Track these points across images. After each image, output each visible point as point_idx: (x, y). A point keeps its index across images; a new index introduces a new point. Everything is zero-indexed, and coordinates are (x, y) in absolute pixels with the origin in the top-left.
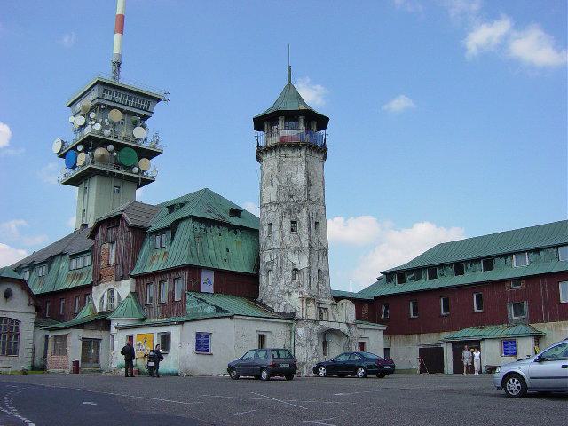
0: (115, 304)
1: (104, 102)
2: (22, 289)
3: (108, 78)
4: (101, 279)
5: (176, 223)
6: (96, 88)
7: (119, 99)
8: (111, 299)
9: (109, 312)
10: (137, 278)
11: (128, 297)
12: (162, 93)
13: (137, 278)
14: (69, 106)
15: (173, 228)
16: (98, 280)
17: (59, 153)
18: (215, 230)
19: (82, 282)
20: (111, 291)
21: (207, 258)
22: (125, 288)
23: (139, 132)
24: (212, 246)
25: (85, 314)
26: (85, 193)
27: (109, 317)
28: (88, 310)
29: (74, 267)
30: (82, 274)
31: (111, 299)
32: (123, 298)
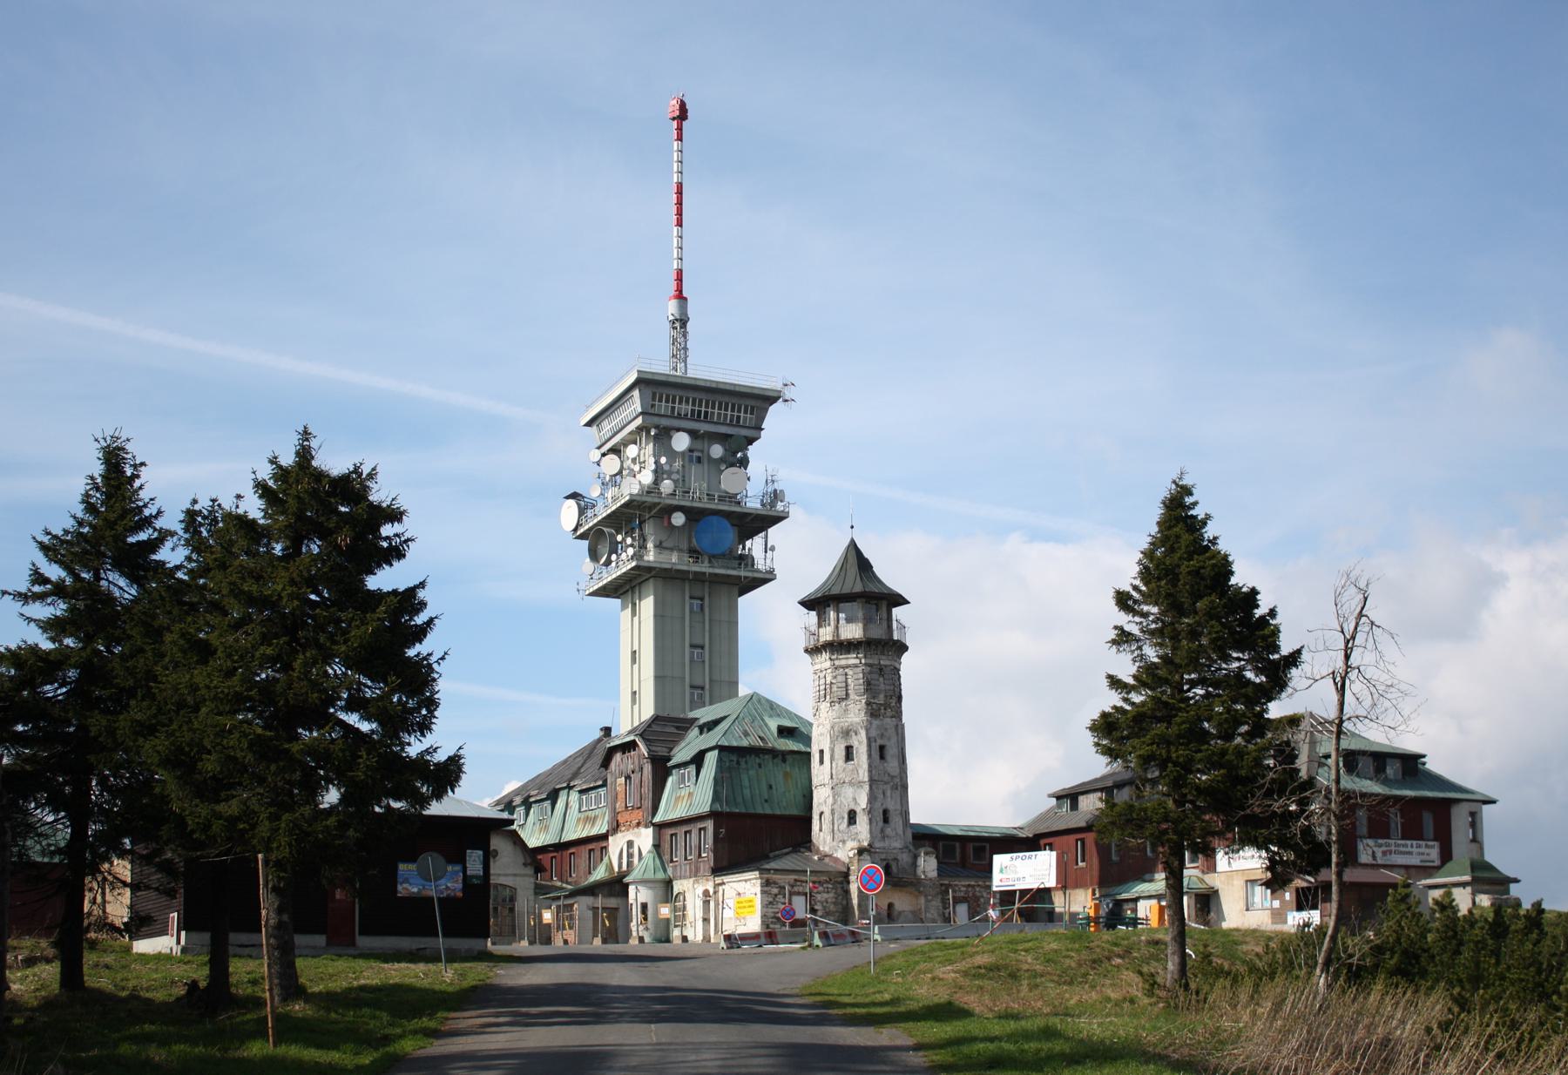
0: (636, 860)
1: (656, 420)
2: (515, 843)
3: (661, 365)
4: (618, 826)
6: (636, 393)
7: (686, 408)
8: (630, 856)
9: (623, 875)
12: (779, 386)
14: (589, 424)
16: (615, 828)
17: (575, 530)
18: (753, 760)
19: (594, 831)
20: (630, 844)
21: (739, 799)
22: (644, 839)
23: (729, 480)
24: (746, 783)
25: (600, 874)
26: (634, 614)
27: (626, 880)
30: (595, 818)
31: (630, 856)
32: (644, 853)
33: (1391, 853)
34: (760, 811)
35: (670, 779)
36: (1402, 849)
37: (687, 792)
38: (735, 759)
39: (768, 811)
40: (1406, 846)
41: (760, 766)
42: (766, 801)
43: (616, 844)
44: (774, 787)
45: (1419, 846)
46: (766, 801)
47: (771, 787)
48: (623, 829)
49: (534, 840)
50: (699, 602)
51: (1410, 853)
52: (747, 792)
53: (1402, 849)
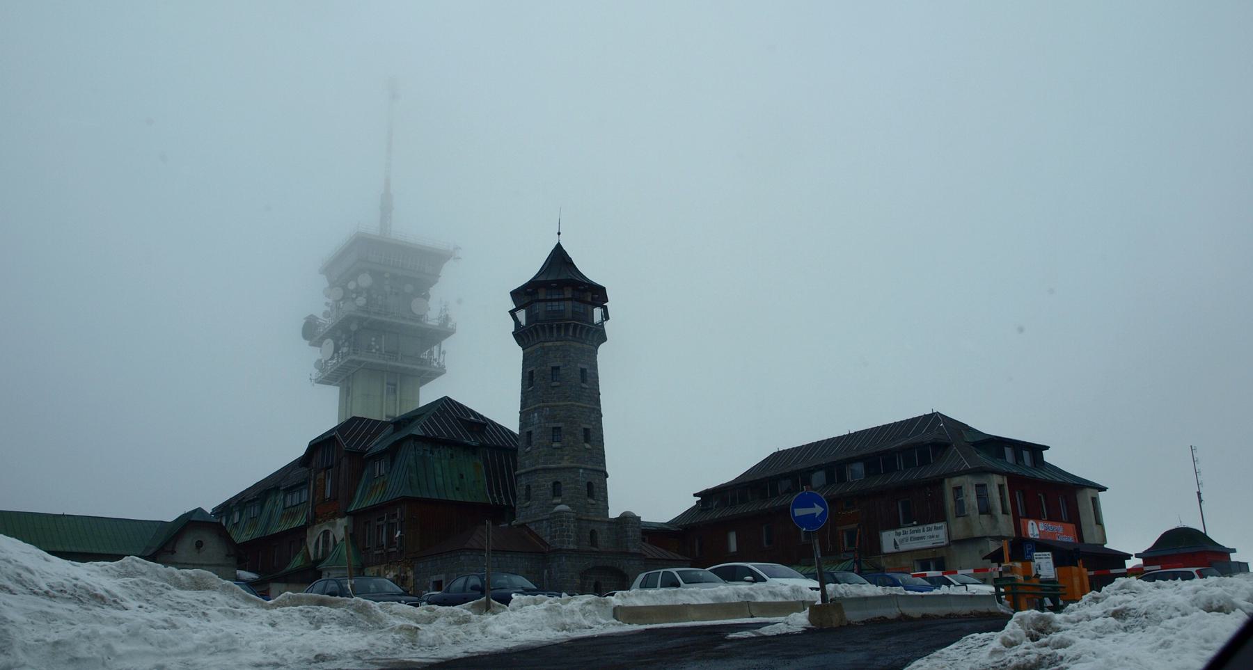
0: (331, 549)
5: (397, 445)
9: (317, 562)
10: (355, 515)
11: (343, 540)
13: (355, 515)
15: (392, 452)
16: (313, 521)
19: (295, 524)
20: (326, 533)
22: (339, 528)
25: (297, 562)
28: (300, 559)
29: (288, 504)
32: (338, 540)
33: (907, 541)
34: (451, 497)
35: (366, 472)
36: (916, 535)
37: (382, 481)
38: (429, 449)
39: (460, 499)
40: (918, 531)
41: (452, 456)
42: (457, 489)
43: (313, 538)
44: (464, 476)
45: (929, 530)
46: (457, 489)
47: (462, 476)
48: (320, 520)
49: (242, 537)
50: (393, 387)
51: (922, 538)
52: (439, 480)
53: (916, 535)
